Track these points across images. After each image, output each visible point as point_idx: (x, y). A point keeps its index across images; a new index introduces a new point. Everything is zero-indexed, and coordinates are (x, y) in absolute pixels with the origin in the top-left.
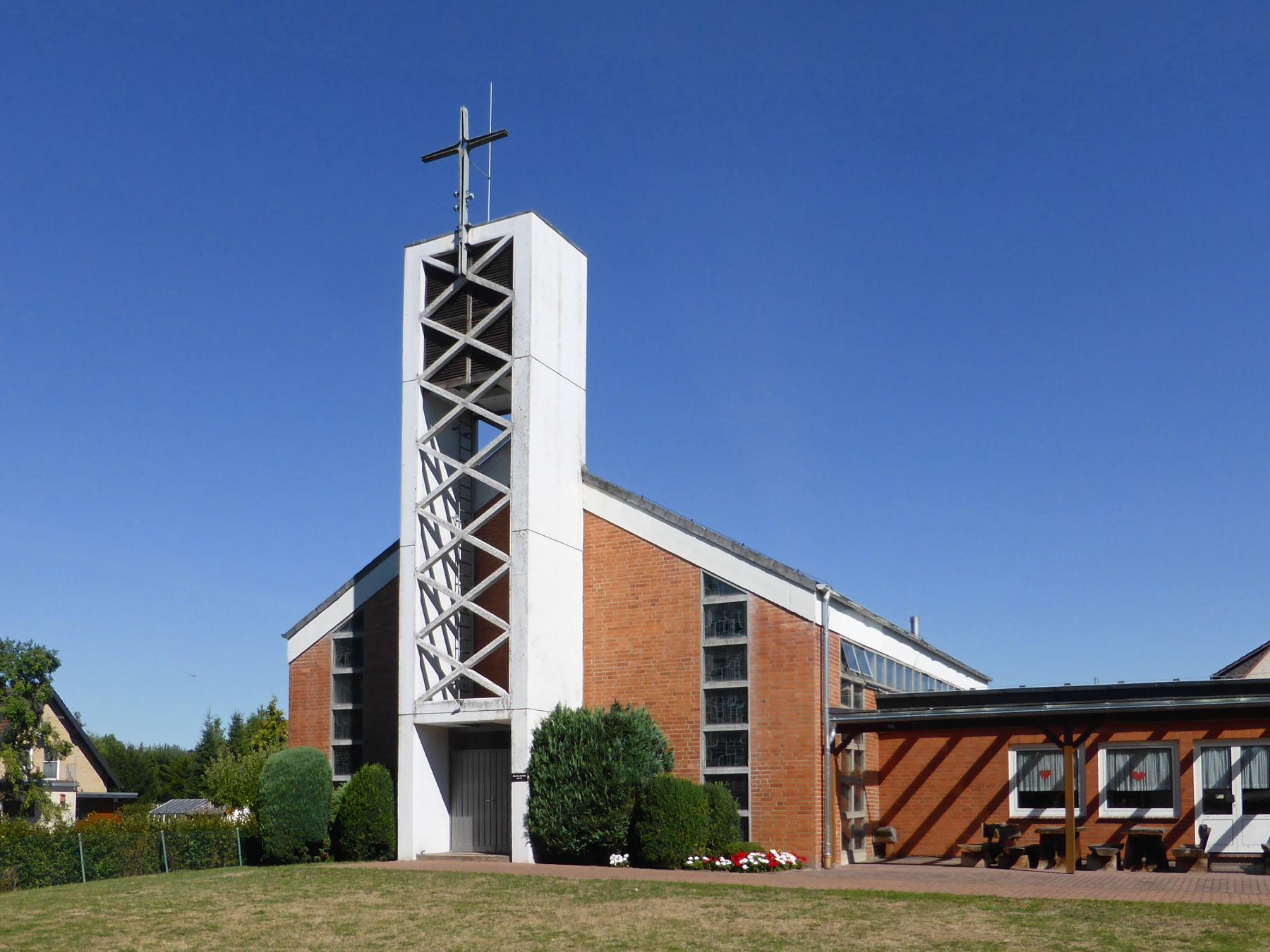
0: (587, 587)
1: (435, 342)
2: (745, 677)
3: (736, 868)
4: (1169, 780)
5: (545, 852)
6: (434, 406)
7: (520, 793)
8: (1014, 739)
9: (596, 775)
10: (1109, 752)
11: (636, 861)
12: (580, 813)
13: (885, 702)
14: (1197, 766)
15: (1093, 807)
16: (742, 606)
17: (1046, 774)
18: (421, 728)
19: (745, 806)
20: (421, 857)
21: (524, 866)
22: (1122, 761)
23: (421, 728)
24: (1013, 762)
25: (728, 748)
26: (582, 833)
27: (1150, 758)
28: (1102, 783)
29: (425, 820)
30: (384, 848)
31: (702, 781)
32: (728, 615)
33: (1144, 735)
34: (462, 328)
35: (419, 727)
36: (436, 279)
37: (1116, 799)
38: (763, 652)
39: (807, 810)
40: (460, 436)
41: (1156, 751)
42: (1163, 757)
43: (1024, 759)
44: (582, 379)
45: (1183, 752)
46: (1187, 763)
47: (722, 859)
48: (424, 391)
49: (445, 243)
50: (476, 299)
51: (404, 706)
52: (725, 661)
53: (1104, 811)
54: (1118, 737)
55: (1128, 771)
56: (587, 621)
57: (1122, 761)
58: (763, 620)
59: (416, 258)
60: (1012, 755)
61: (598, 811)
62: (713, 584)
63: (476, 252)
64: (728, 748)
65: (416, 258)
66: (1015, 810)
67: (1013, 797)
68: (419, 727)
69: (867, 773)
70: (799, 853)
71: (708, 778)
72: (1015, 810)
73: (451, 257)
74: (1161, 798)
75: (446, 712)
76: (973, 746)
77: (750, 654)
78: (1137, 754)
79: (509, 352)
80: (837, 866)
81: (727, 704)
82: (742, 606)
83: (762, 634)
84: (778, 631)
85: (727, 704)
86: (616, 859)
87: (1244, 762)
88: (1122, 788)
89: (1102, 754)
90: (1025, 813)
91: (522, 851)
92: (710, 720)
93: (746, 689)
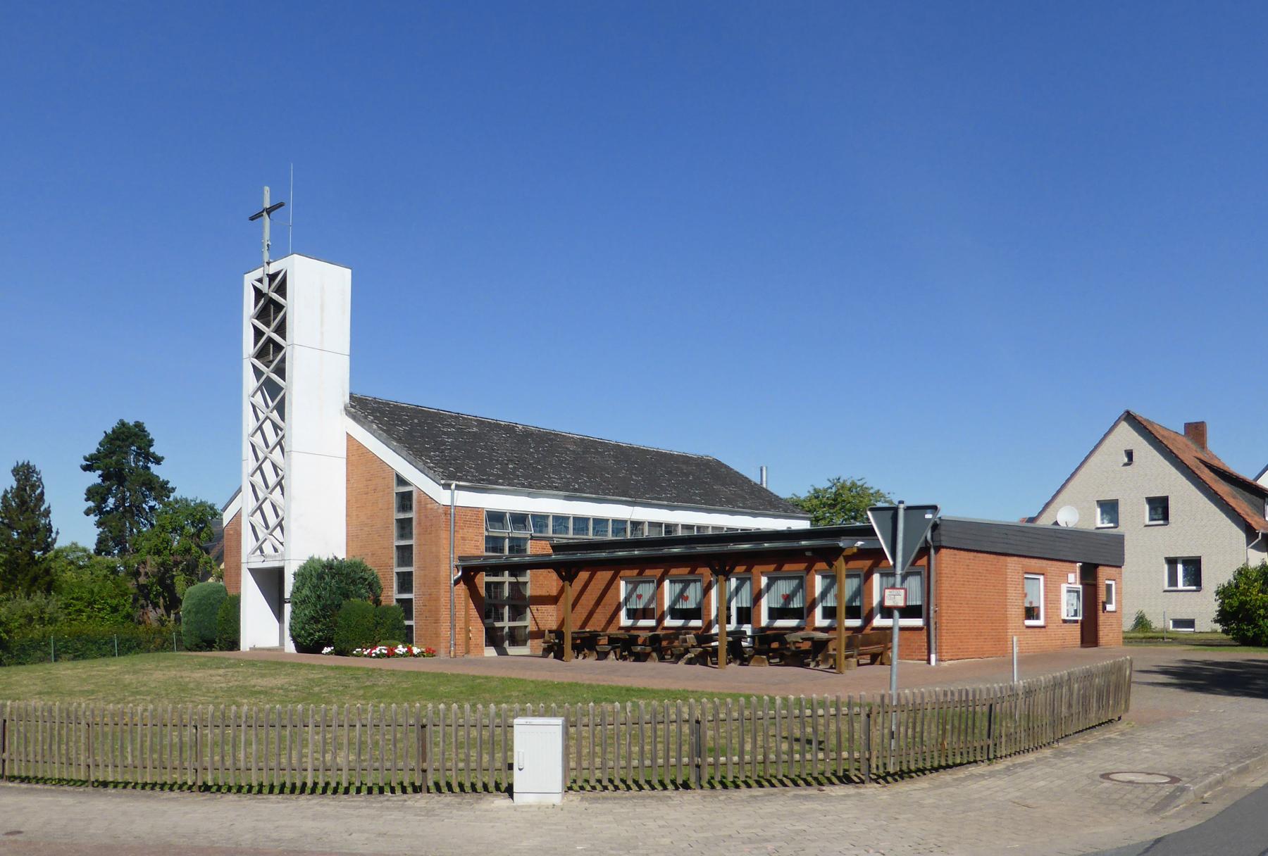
0: (348, 480)
1: (258, 333)
2: (411, 538)
3: (370, 655)
4: (700, 603)
5: (301, 648)
6: (258, 373)
7: (288, 608)
8: (622, 573)
9: (313, 600)
10: (671, 582)
11: (339, 652)
12: (309, 623)
13: (556, 548)
14: (714, 593)
15: (660, 620)
16: (411, 493)
17: (640, 597)
18: (252, 571)
19: (410, 618)
20: (254, 649)
21: (290, 655)
22: (678, 587)
23: (254, 572)
24: (623, 587)
25: (405, 582)
26: (310, 634)
27: (692, 585)
28: (667, 604)
29: (261, 627)
30: (234, 644)
31: (394, 603)
32: (405, 501)
33: (687, 570)
34: (268, 325)
35: (251, 570)
36: (259, 294)
37: (675, 613)
38: (419, 523)
39: (437, 621)
40: (272, 389)
41: (695, 581)
42: (698, 584)
43: (630, 586)
44: (347, 351)
45: (706, 580)
46: (706, 591)
47: (400, 647)
48: (254, 366)
49: (258, 273)
50: (271, 308)
51: (244, 559)
52: (405, 527)
53: (668, 622)
54: (674, 571)
55: (681, 596)
56: (348, 501)
57: (678, 587)
58: (419, 502)
59: (250, 279)
60: (623, 583)
61: (317, 622)
62: (401, 481)
63: (272, 277)
64: (405, 582)
65: (250, 279)
66: (624, 621)
67: (623, 613)
68: (251, 570)
69: (531, 597)
70: (433, 648)
71: (398, 600)
72: (624, 621)
73: (260, 281)
74: (696, 613)
75: (258, 563)
76: (603, 576)
77: (414, 523)
78: (686, 583)
79: (284, 338)
80: (470, 657)
81: (405, 554)
82: (411, 493)
83: (419, 512)
84: (426, 509)
85: (405, 554)
86: (326, 650)
87: (738, 589)
88: (677, 607)
89: (667, 583)
90: (629, 623)
91: (290, 647)
92: (399, 565)
93: (411, 546)
